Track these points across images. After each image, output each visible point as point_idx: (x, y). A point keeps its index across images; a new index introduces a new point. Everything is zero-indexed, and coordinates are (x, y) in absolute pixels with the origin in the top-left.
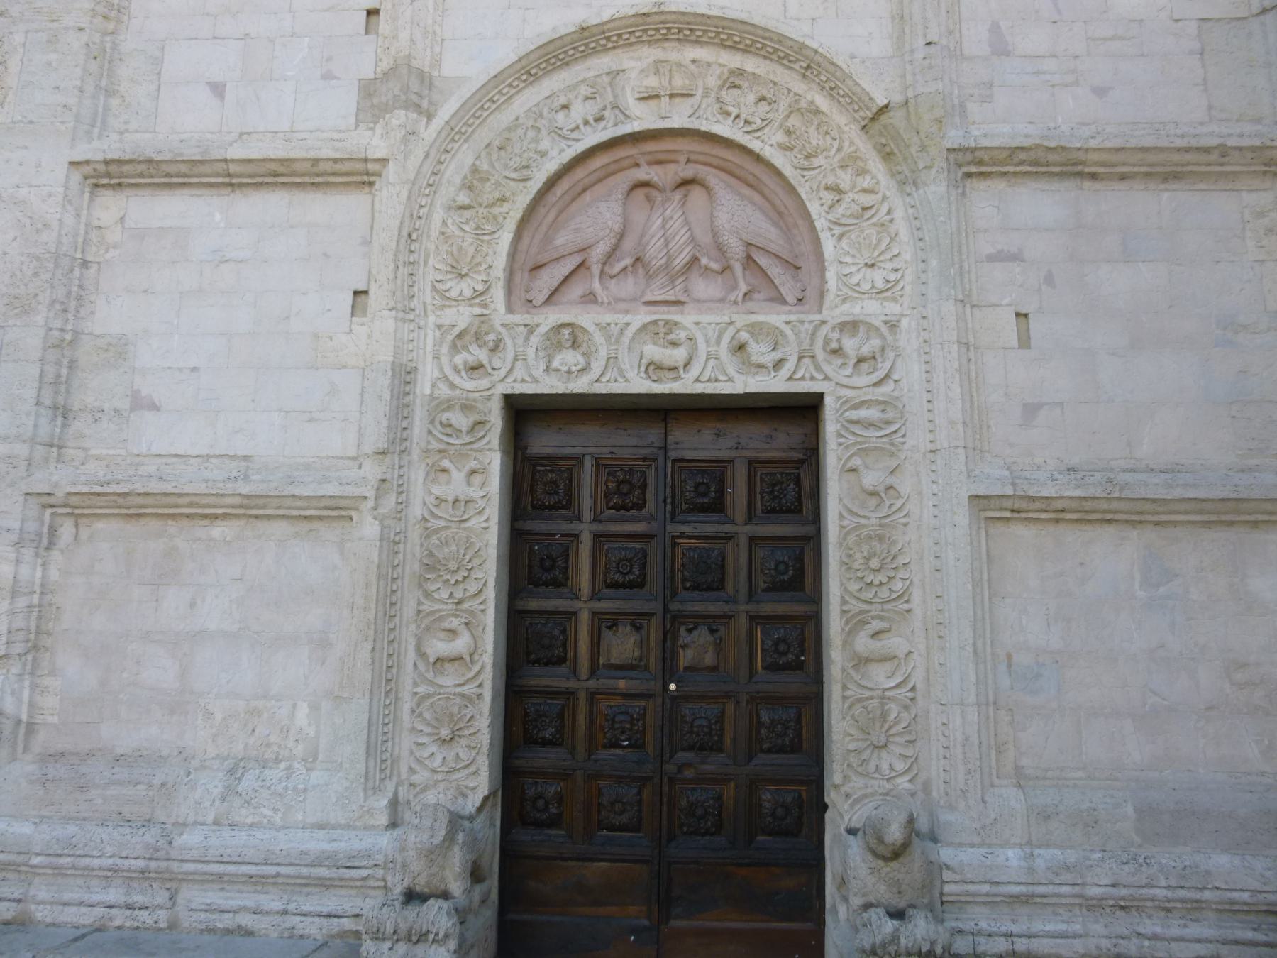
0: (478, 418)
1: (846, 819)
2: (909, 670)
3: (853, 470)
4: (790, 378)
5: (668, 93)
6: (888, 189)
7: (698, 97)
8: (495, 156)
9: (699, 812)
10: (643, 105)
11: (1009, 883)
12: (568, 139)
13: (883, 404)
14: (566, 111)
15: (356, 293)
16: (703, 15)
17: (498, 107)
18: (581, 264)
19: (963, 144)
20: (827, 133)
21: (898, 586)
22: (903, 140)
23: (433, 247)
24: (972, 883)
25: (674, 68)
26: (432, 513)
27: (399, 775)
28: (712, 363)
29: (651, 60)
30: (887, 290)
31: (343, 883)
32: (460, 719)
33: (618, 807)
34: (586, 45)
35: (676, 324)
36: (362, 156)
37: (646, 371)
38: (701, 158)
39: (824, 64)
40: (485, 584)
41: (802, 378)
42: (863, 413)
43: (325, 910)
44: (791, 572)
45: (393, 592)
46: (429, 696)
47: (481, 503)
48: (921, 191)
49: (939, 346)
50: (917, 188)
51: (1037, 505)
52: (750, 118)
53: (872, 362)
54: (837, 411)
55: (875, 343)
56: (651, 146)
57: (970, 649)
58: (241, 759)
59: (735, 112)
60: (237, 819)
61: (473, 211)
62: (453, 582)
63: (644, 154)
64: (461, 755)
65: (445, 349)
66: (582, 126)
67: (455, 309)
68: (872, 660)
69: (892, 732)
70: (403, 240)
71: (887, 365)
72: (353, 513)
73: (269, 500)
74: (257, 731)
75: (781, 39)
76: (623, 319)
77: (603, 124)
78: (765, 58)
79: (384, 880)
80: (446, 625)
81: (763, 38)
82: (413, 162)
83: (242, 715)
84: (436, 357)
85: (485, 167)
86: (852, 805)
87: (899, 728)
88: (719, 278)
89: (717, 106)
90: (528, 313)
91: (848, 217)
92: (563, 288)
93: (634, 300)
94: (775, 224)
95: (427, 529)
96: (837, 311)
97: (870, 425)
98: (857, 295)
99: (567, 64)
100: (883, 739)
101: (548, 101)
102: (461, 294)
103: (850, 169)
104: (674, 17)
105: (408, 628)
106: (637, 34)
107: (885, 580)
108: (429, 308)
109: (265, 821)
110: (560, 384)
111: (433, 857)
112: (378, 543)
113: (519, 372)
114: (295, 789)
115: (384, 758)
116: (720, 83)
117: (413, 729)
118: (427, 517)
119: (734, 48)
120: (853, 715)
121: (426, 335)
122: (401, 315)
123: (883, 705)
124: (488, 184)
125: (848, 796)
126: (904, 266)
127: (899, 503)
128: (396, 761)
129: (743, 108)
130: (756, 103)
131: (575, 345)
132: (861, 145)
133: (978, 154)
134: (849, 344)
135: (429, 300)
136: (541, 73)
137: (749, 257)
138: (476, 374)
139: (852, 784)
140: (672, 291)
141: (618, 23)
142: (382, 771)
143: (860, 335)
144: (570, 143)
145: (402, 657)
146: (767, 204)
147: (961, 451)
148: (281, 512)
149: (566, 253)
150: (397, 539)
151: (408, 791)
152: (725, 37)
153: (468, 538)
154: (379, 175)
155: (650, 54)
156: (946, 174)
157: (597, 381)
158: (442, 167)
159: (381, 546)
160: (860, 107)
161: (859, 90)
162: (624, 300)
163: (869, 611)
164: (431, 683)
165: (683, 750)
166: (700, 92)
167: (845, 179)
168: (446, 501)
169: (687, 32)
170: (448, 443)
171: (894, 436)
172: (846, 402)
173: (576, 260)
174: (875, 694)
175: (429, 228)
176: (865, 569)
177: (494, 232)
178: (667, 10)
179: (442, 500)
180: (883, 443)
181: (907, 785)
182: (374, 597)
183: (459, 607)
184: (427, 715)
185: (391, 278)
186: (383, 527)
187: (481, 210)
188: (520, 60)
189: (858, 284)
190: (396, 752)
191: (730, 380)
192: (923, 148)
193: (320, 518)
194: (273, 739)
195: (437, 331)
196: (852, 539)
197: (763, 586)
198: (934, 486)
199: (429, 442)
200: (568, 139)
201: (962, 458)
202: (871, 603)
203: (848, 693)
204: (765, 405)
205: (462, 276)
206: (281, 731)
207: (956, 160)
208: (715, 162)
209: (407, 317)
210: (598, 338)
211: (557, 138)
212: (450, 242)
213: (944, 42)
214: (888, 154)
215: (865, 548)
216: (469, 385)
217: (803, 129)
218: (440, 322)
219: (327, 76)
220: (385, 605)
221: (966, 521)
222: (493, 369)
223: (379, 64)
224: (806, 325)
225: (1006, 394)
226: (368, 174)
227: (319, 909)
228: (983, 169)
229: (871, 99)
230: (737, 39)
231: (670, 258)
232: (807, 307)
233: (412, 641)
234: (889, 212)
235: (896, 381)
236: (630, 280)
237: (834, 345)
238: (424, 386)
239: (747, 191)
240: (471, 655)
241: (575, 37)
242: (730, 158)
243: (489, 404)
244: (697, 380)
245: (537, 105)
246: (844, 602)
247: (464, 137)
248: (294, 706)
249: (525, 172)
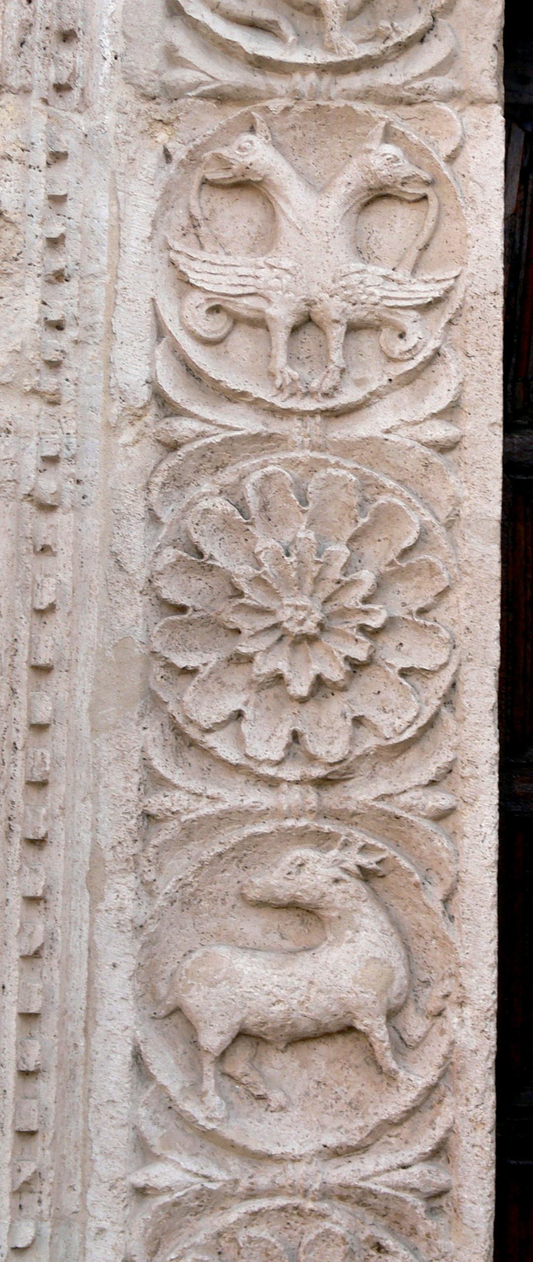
26: (192, 372)
40: (449, 698)
62: (301, 688)
95: (173, 447)
105: (96, 897)
118: (176, 394)
150: (48, 485)
168: (259, 323)
170: (260, 64)
179: (236, 320)
183: (333, 798)
199: (172, 57)
240: (392, 1014)
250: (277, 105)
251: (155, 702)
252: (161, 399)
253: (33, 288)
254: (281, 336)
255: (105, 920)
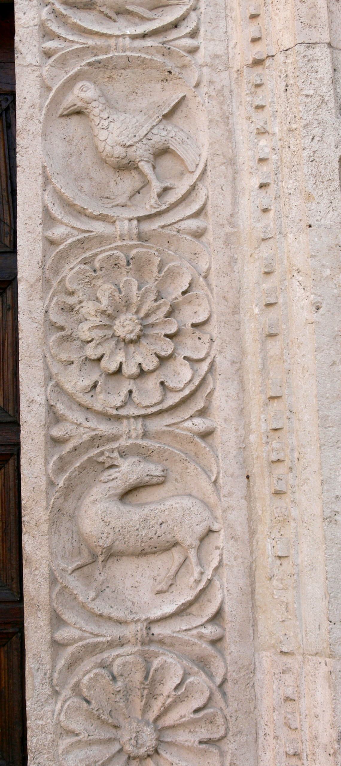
2: (209, 574)
3: (78, 113)
68: (121, 554)
107: (150, 364)
120: (77, 685)
123: (147, 660)
163: (115, 438)
171: (174, 34)
174: (128, 631)
176: (105, 339)
180: (146, 49)
202: (118, 418)
203: (63, 634)
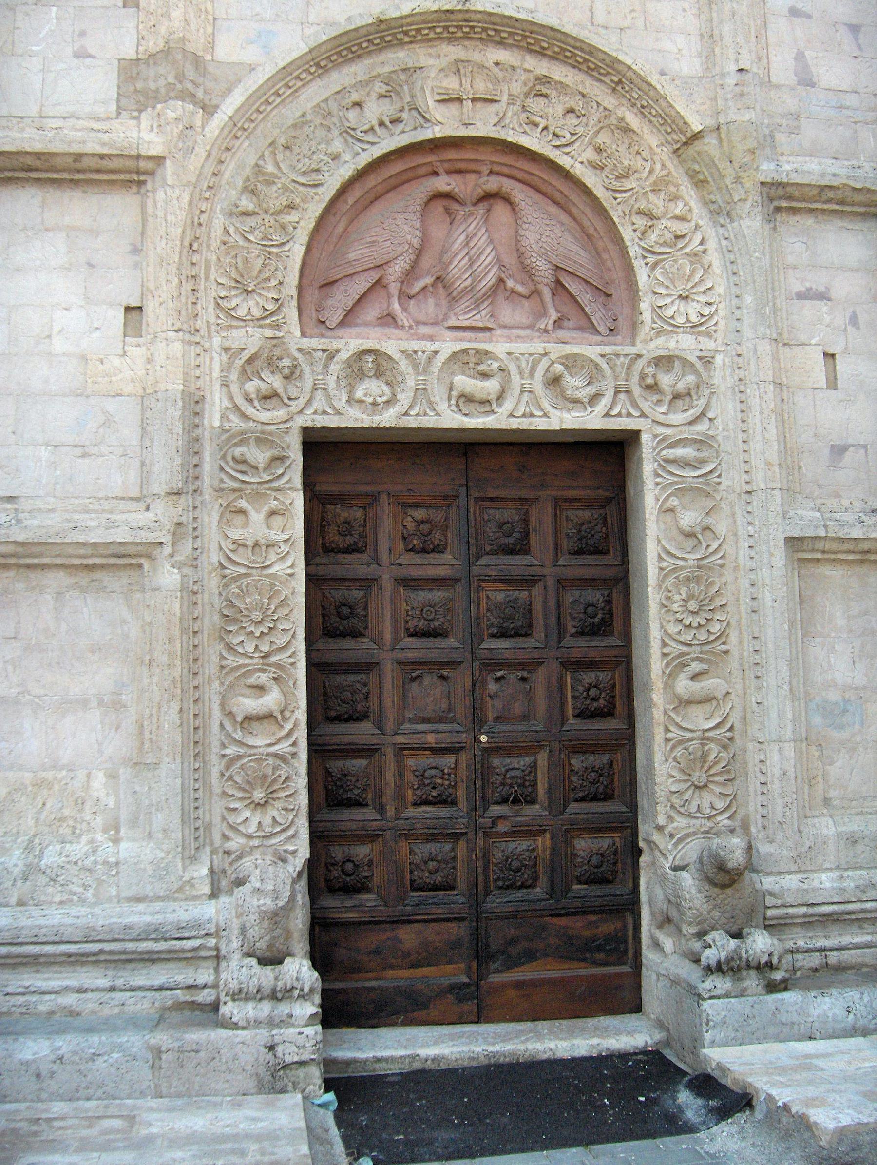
0: (276, 452)
1: (671, 858)
4: (607, 415)
5: (471, 96)
6: (701, 218)
7: (504, 104)
8: (280, 157)
9: (515, 864)
10: (443, 108)
11: (824, 903)
12: (362, 141)
13: (700, 443)
14: (357, 109)
15: (128, 309)
16: (511, 18)
17: (283, 101)
18: (378, 282)
19: (776, 178)
20: (638, 153)
21: (716, 628)
22: (718, 170)
23: (214, 258)
24: (792, 906)
25: (475, 69)
26: (229, 559)
27: (212, 844)
28: (526, 397)
29: (453, 57)
30: (701, 324)
31: (172, 956)
32: (274, 781)
33: (432, 865)
34: (382, 38)
35: (487, 353)
36: (134, 152)
37: (457, 405)
38: (506, 170)
39: (637, 81)
40: (293, 636)
41: (619, 415)
42: (679, 452)
43: (157, 983)
44: (600, 616)
45: (195, 646)
46: (239, 757)
47: (285, 548)
48: (735, 224)
49: (756, 386)
50: (732, 221)
51: (846, 547)
52: (558, 131)
53: (687, 399)
54: (654, 449)
55: (691, 379)
56: (452, 154)
57: (786, 687)
58: (35, 836)
59: (543, 123)
60: (43, 898)
61: (259, 219)
63: (441, 161)
64: (277, 819)
65: (234, 376)
66: (377, 128)
67: (243, 330)
69: (712, 772)
70: (185, 250)
71: (702, 402)
72: (142, 561)
73: (48, 547)
74: (48, 805)
75: (592, 50)
76: (430, 347)
77: (401, 127)
78: (574, 67)
79: (217, 949)
80: (252, 681)
81: (573, 47)
82: (195, 162)
83: (30, 788)
84: (225, 385)
85: (270, 168)
86: (676, 845)
87: (718, 768)
88: (526, 303)
89: (524, 115)
90: (322, 336)
91: (661, 245)
92: (357, 308)
93: (436, 323)
94: (583, 247)
95: (225, 577)
96: (652, 345)
97: (686, 464)
98: (670, 328)
99: (359, 56)
100: (704, 779)
101: (338, 97)
102: (249, 313)
103: (662, 196)
104: (479, 16)
105: (210, 687)
106: (438, 30)
107: (703, 622)
108: (213, 327)
109: (75, 898)
110: (365, 416)
111: (278, 919)
112: (179, 594)
113: (319, 403)
114: (105, 863)
115: (197, 825)
116: (526, 89)
117: (224, 793)
118: (225, 564)
119: (541, 53)
121: (211, 359)
122: (187, 337)
123: (703, 745)
124: (275, 188)
125: (672, 836)
126: (718, 299)
127: (715, 546)
128: (208, 827)
129: (550, 119)
130: (564, 115)
131: (379, 374)
132: (673, 170)
133: (788, 189)
134: (666, 380)
135: (212, 320)
136: (330, 65)
137: (558, 282)
138: (269, 404)
139: (675, 824)
140: (478, 317)
141: (417, 18)
142: (196, 839)
143: (676, 370)
144: (365, 146)
145: (206, 717)
146: (573, 224)
147: (777, 493)
148: (59, 561)
149: (360, 269)
150: (196, 588)
151: (223, 860)
152: (532, 42)
153: (272, 585)
154: (152, 173)
155: (452, 52)
156: (760, 207)
157: (406, 414)
158: (223, 167)
159: (182, 597)
160: (673, 130)
161: (673, 113)
162: (425, 324)
163: (688, 654)
164: (242, 744)
165: (497, 803)
166: (505, 98)
167: (657, 203)
168: (245, 546)
169: (492, 33)
170: (243, 482)
172: (663, 440)
173: (374, 276)
175: (209, 238)
177: (283, 244)
178: (472, 8)
180: (699, 483)
181: (727, 822)
182: (179, 653)
183: (266, 661)
184: (238, 779)
185: (175, 295)
186: (183, 576)
187: (267, 218)
188: (310, 51)
189: (672, 317)
190: (207, 819)
191: (545, 415)
192: (738, 180)
193: (102, 567)
194: (67, 812)
195: (223, 353)
196: (670, 581)
197: (573, 630)
198: (750, 528)
199: (222, 481)
200: (362, 141)
201: (778, 500)
203: (670, 735)
204: (572, 440)
205: (248, 292)
206: (76, 804)
207: (768, 193)
208: (519, 175)
209: (193, 339)
210: (404, 365)
211: (350, 140)
212: (233, 254)
213: (755, 70)
214: (702, 182)
215: (684, 590)
216: (265, 416)
217: (614, 147)
218: (227, 344)
219: (81, 54)
220: (188, 661)
221: (783, 562)
222: (290, 399)
223: (143, 42)
224: (622, 359)
225: (815, 435)
226: (138, 172)
227: (148, 983)
228: (794, 204)
229: (685, 123)
230: (545, 45)
231: (476, 280)
232: (619, 338)
233: (216, 701)
234: (702, 243)
235: (710, 419)
236: (431, 301)
237: (650, 381)
238: (213, 418)
239: (553, 209)
240: (282, 712)
241: (372, 29)
242: (537, 172)
243: (287, 438)
244: (511, 415)
245: (327, 100)
246: (664, 645)
247: (246, 133)
248: (89, 775)
249: (314, 176)
250: (247, 492)
251: (222, 639)
252: (221, 564)
253: (191, 540)
254: (250, 549)
255: (213, 691)
